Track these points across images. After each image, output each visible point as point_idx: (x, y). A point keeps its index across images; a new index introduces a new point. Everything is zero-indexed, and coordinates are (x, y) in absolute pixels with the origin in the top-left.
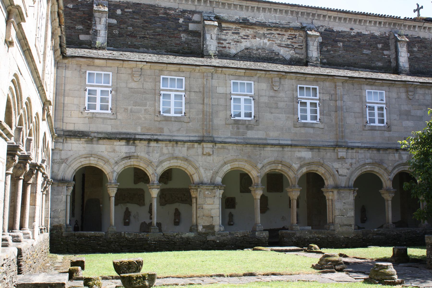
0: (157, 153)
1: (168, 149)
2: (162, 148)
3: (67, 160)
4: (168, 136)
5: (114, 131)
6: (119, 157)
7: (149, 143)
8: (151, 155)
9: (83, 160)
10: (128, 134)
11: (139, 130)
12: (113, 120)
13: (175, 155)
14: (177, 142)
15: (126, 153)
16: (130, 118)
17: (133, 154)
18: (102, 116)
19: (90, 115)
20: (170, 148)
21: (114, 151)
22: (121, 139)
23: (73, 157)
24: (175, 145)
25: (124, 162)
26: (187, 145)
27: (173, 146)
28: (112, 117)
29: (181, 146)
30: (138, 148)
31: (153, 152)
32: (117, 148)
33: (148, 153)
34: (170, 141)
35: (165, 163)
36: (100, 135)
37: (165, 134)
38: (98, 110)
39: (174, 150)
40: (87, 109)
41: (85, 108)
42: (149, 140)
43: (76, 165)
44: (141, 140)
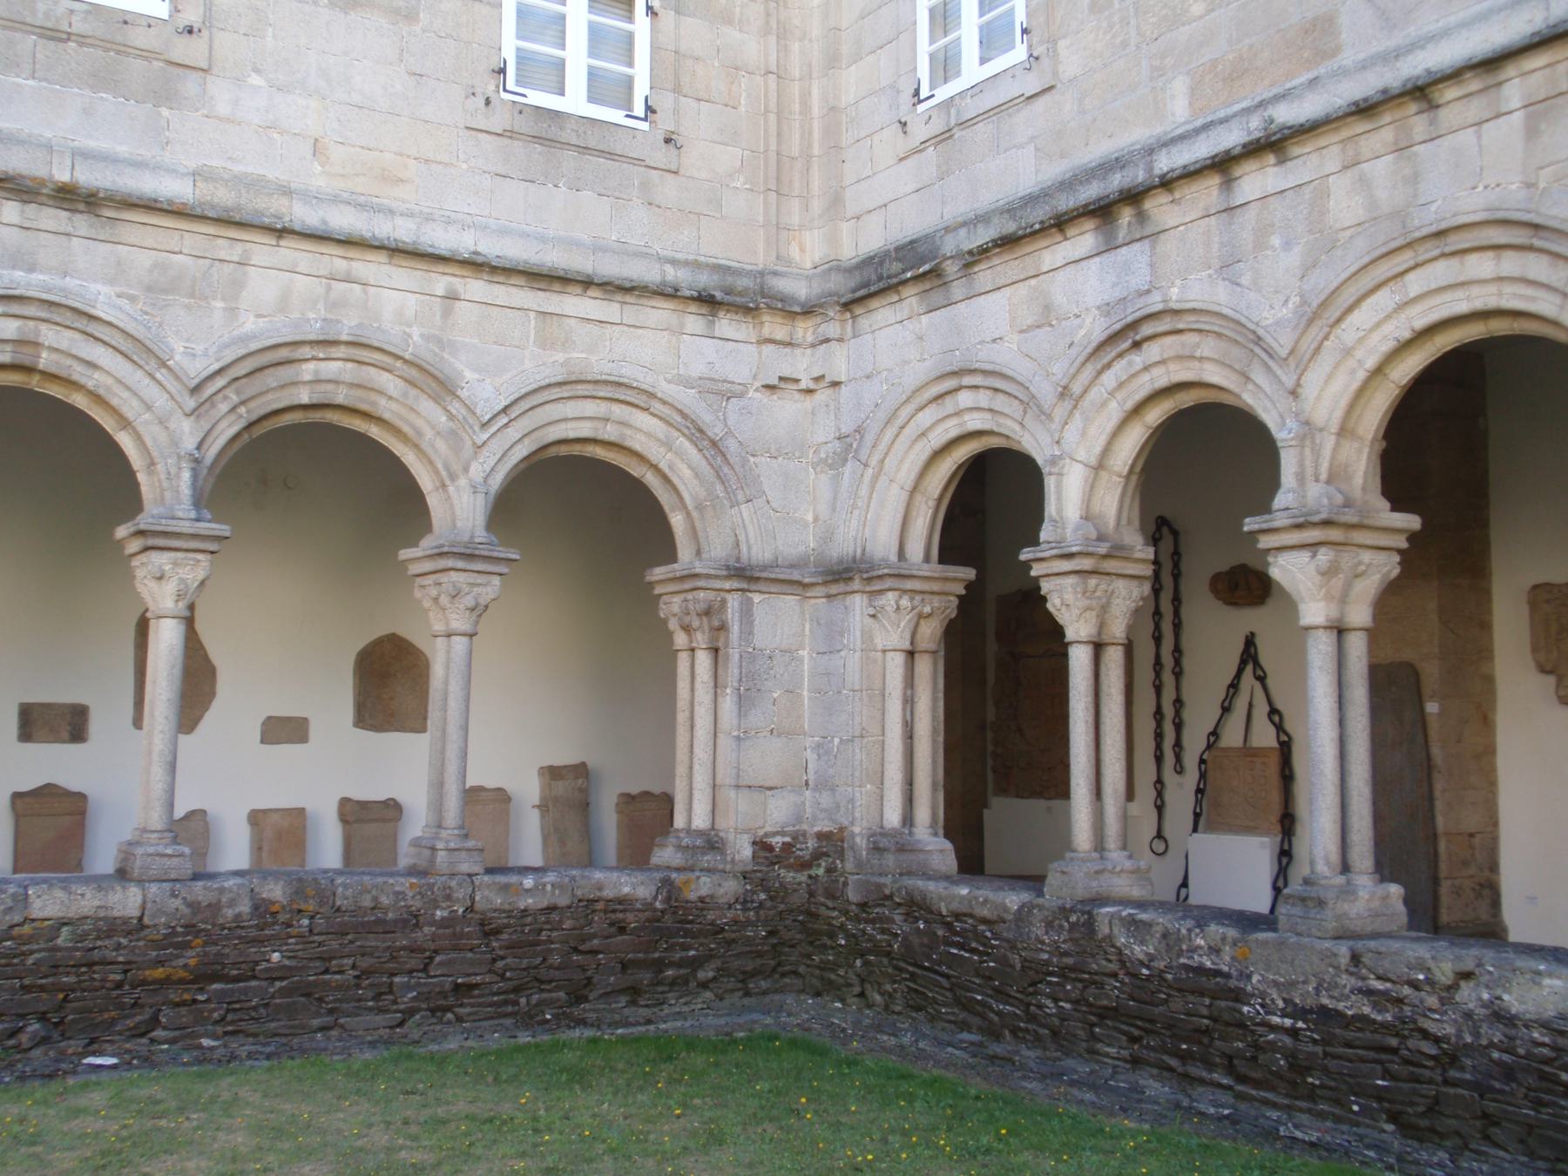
0: (1287, 245)
1: (1364, 183)
2: (1323, 194)
3: (862, 437)
4: (1363, 66)
5: (1054, 170)
6: (1074, 351)
7: (1228, 183)
8: (1245, 280)
9: (926, 417)
10: (1117, 163)
11: (1179, 110)
12: (1040, 103)
13: (1426, 220)
14: (1421, 92)
15: (1106, 309)
16: (1125, 44)
17: (1140, 303)
18: (988, 100)
19: (937, 126)
20: (1381, 169)
21: (1047, 316)
22: (1060, 224)
23: (882, 415)
24: (1419, 125)
25: (1109, 379)
26: (1516, 87)
27: (1401, 149)
28: (1031, 84)
29: (1476, 109)
30: (1168, 244)
31: (1260, 244)
32: (1060, 289)
33: (1227, 267)
34: (1364, 110)
35: (1362, 317)
36: (981, 229)
37: (1348, 58)
38: (972, 71)
39: (1415, 179)
40: (924, 94)
41: (917, 93)
42: (1223, 165)
43: (905, 462)
44: (1167, 183)
